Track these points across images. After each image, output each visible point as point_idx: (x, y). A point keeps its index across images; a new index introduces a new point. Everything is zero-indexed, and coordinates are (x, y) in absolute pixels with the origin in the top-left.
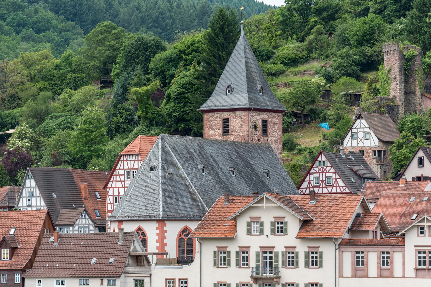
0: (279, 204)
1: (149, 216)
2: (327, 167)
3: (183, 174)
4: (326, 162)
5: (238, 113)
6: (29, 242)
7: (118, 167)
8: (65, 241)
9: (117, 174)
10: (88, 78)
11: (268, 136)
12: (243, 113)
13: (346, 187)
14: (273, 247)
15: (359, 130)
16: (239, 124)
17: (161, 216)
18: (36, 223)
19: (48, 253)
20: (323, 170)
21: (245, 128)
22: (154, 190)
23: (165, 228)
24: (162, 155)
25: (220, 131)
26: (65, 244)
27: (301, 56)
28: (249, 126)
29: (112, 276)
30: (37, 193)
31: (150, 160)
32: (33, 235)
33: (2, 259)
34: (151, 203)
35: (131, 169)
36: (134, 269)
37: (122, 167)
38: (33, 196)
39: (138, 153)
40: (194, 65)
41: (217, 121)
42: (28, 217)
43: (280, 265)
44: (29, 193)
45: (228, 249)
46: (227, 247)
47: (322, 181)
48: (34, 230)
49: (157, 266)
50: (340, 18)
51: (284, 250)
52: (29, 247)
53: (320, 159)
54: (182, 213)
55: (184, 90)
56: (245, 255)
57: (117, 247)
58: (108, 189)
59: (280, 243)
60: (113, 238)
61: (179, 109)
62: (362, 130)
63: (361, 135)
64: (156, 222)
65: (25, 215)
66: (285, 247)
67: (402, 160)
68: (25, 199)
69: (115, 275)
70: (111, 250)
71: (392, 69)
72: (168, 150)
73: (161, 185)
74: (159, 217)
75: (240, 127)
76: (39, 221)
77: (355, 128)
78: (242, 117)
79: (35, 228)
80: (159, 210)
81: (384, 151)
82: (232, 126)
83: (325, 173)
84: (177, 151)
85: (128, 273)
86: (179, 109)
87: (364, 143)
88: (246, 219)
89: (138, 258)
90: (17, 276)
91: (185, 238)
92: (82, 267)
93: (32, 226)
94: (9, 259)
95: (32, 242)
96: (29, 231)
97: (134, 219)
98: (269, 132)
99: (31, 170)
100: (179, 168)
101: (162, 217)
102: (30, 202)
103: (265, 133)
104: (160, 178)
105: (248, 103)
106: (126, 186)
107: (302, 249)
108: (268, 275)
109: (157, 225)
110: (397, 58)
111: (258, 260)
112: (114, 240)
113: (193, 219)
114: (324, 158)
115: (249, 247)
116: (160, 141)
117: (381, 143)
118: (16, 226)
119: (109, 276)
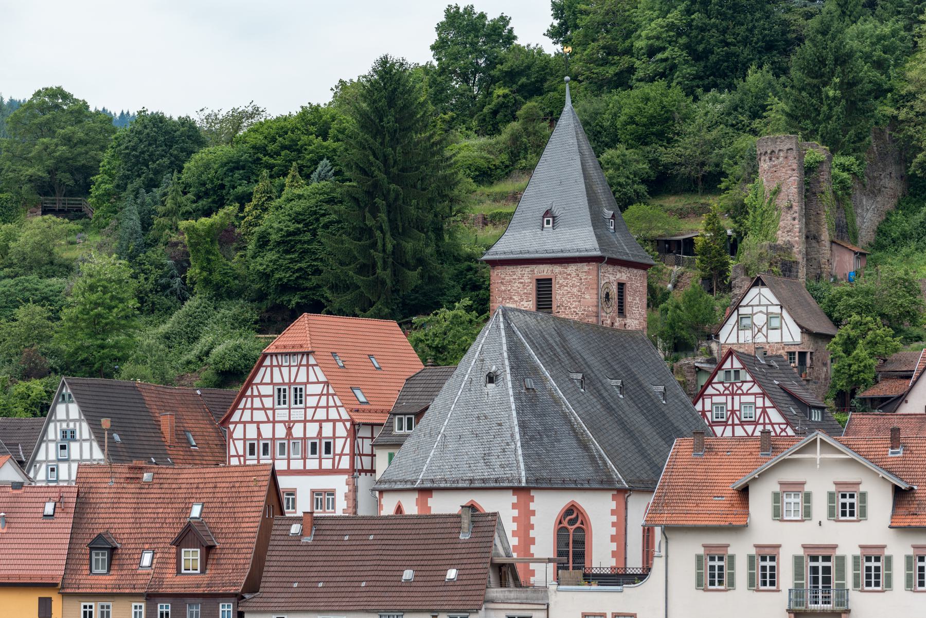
0: (851, 455)
1: (496, 481)
2: (743, 382)
3: (556, 390)
4: (742, 372)
5: (572, 269)
6: (241, 535)
7: (257, 380)
8: (328, 533)
9: (256, 393)
10: (16, 202)
11: (625, 317)
12: (585, 267)
13: (787, 424)
14: (834, 547)
15: (756, 309)
16: (575, 290)
17: (524, 480)
18: (249, 494)
19: (292, 559)
20: (735, 388)
21: (590, 298)
22: (500, 425)
23: (532, 506)
24: (510, 349)
25: (530, 304)
26: (329, 538)
27: (497, 162)
28: (597, 294)
29: (461, 607)
30: (84, 430)
31: (483, 360)
32: (247, 520)
33: (183, 571)
34: (496, 450)
35: (290, 384)
36: (507, 594)
37: (267, 379)
38: (73, 438)
39: (310, 349)
40: (294, 176)
41: (521, 283)
42: (228, 479)
43: (849, 582)
44: (64, 433)
45: (730, 551)
46: (727, 546)
47: (733, 412)
48: (248, 509)
49: (561, 587)
50: (555, 90)
51: (858, 552)
52: (242, 546)
53: (727, 365)
54: (565, 474)
55: (301, 226)
56: (768, 564)
57: (459, 546)
58: (232, 427)
59: (848, 539)
60: (445, 526)
61: (291, 266)
62: (764, 309)
63: (760, 320)
64: (511, 492)
65: (220, 475)
66: (862, 547)
67: (859, 372)
68: (52, 446)
69: (469, 607)
70: (445, 552)
71: (784, 189)
72: (520, 340)
73: (514, 413)
74: (520, 482)
75: (577, 296)
76: (256, 489)
77: (747, 306)
78: (583, 276)
79: (249, 504)
80: (518, 467)
81: (811, 353)
82: (559, 295)
83: (740, 395)
84: (532, 341)
85: (493, 602)
86: (291, 266)
87: (767, 337)
88: (771, 486)
89: (503, 569)
90: (226, 609)
91: (569, 527)
92: (382, 589)
93: (242, 499)
94: (199, 571)
95: (246, 535)
96: (236, 510)
97: (460, 485)
98: (627, 308)
99: (70, 384)
100: (546, 378)
101: (527, 482)
102: (65, 452)
103: (621, 311)
104: (512, 399)
105: (597, 246)
106: (277, 419)
107: (899, 550)
108: (820, 606)
109: (514, 499)
110: (795, 166)
111: (798, 574)
112: (449, 531)
113: (587, 486)
114: (737, 365)
115: (779, 546)
116: (501, 319)
117: (806, 337)
118: (205, 500)
119: (454, 607)
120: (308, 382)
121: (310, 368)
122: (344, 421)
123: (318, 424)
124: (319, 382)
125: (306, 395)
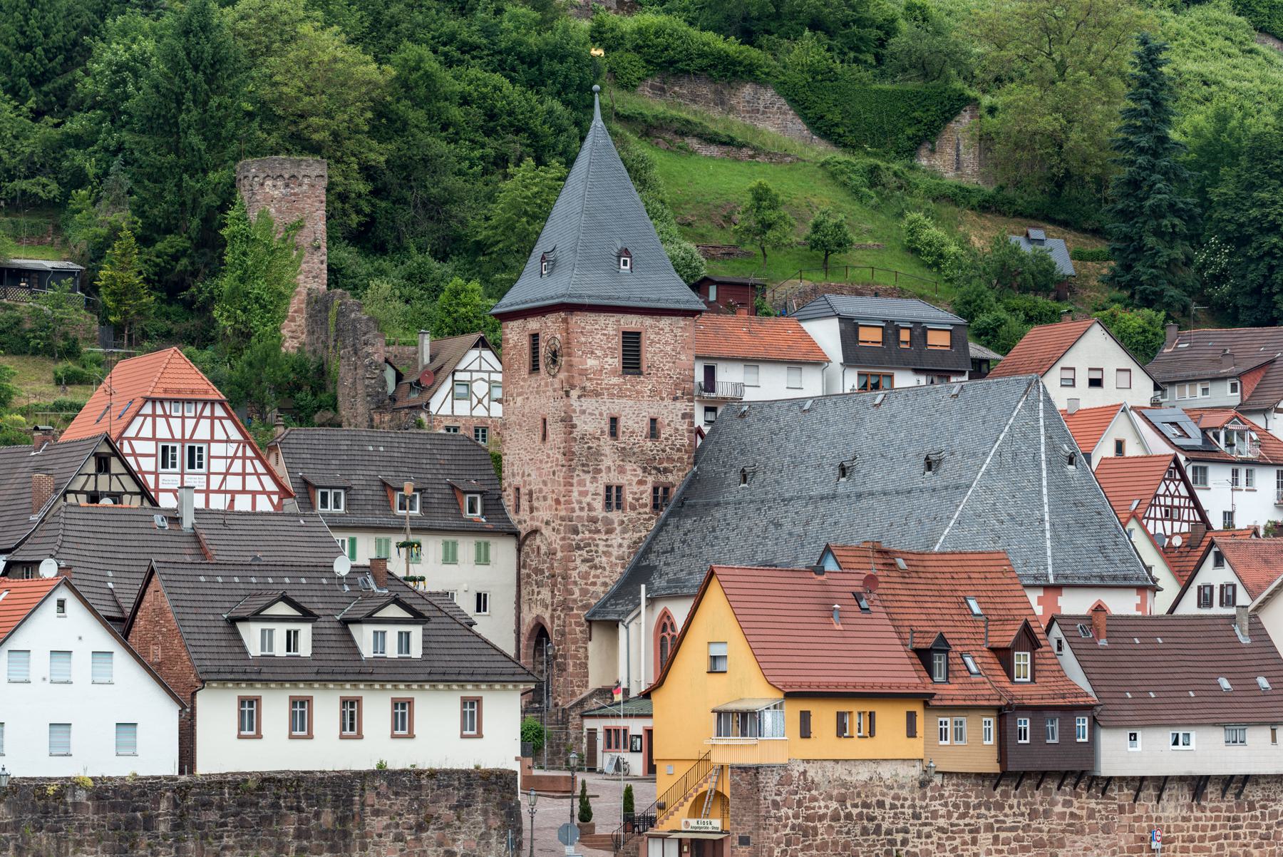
16: (669, 348)
25: (615, 362)
37: (146, 432)
82: (649, 354)
120: (213, 440)
121: (217, 422)
122: (269, 494)
123: (229, 496)
124: (228, 441)
125: (210, 457)
